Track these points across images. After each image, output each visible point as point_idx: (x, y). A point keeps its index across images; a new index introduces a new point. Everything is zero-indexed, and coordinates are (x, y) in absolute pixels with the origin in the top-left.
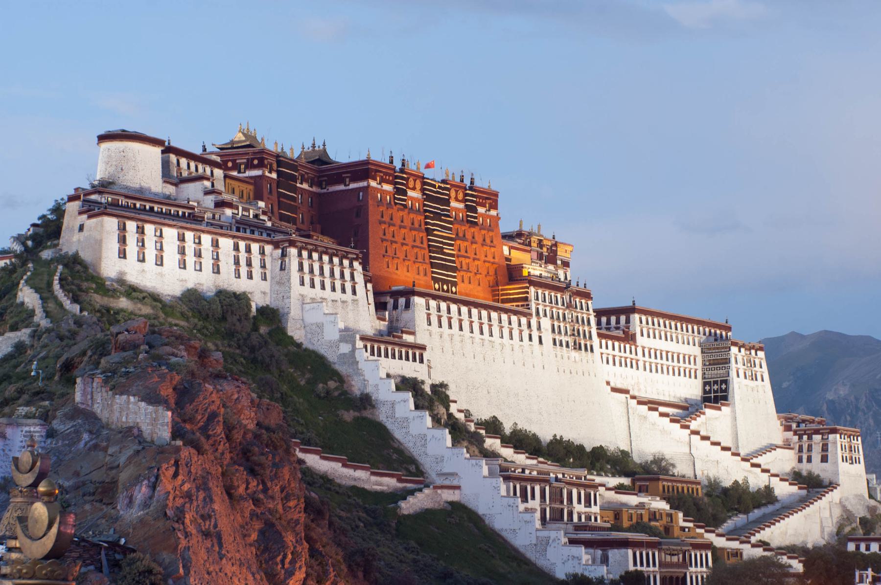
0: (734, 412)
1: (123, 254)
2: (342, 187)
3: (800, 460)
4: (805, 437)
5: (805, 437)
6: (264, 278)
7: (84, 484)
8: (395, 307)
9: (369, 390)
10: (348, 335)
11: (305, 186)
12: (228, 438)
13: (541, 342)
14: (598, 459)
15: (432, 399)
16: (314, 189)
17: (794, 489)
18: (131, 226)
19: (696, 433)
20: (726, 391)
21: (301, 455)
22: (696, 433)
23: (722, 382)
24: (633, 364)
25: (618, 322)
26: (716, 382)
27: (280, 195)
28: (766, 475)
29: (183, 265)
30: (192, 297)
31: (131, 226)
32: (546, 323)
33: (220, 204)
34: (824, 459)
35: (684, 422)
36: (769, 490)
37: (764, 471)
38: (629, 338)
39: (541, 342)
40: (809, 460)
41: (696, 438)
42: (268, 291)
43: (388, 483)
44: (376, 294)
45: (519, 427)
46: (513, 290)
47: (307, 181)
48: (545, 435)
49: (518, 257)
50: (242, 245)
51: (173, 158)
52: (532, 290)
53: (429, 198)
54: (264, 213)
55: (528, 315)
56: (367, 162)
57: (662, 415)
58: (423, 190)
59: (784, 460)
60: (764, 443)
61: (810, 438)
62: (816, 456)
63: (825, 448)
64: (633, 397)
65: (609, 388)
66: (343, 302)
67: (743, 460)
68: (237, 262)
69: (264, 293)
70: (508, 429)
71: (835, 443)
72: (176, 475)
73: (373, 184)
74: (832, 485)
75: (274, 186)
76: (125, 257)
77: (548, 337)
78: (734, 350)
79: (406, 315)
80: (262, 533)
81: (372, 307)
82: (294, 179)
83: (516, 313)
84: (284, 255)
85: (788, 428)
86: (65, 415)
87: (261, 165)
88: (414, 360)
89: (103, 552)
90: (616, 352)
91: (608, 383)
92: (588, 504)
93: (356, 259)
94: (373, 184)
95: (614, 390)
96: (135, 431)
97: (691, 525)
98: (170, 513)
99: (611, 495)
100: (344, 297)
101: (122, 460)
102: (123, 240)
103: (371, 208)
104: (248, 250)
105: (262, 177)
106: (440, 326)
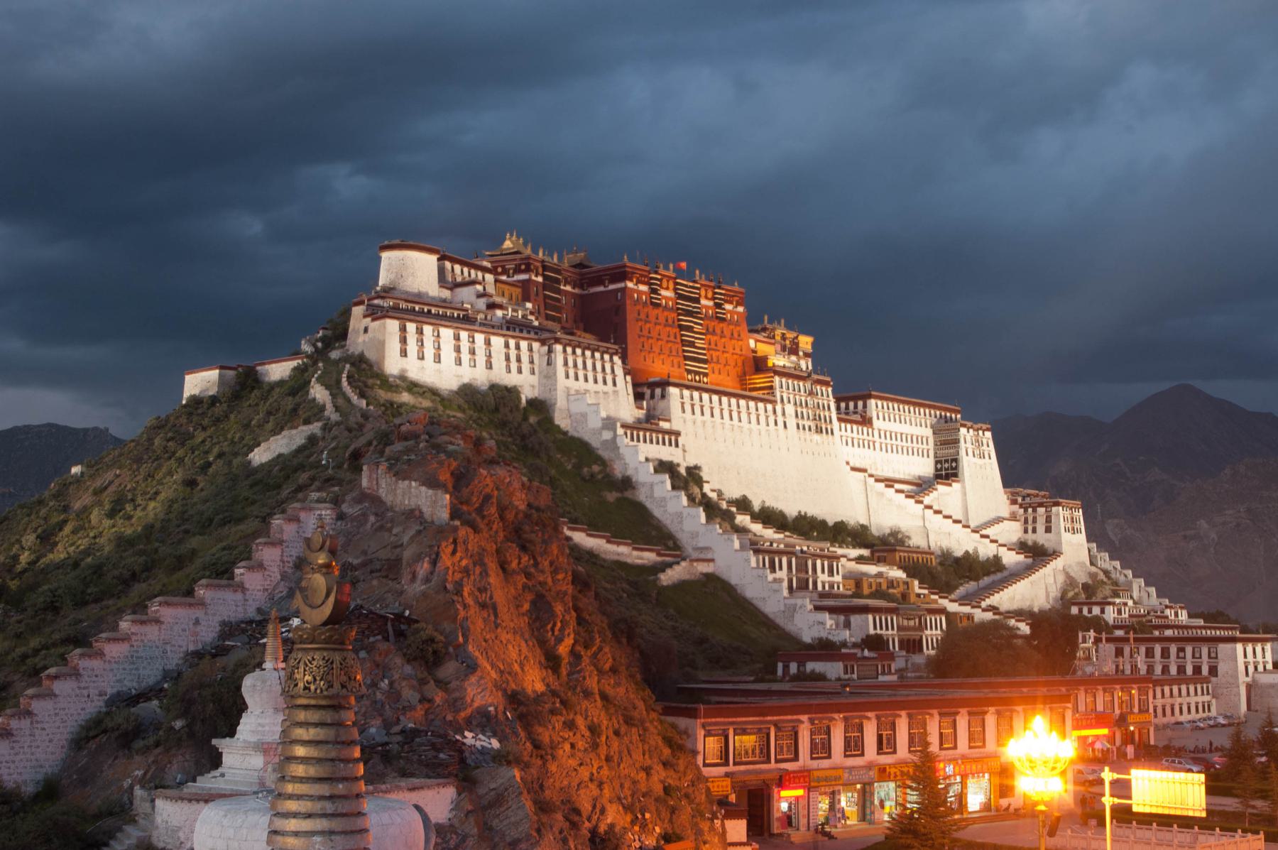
0: (964, 488)
1: (404, 353)
2: (601, 289)
3: (1026, 531)
4: (1030, 510)
5: (1030, 510)
6: (533, 373)
7: (371, 561)
8: (652, 397)
9: (629, 472)
10: (609, 423)
11: (568, 288)
12: (502, 518)
14: (840, 533)
15: (688, 480)
16: (576, 291)
17: (1021, 558)
18: (411, 327)
19: (929, 507)
20: (956, 468)
21: (568, 533)
22: (929, 507)
23: (953, 460)
24: (871, 445)
25: (856, 407)
26: (946, 461)
27: (546, 297)
28: (995, 545)
29: (459, 362)
30: (467, 392)
31: (411, 327)
32: (790, 409)
33: (492, 306)
34: (1048, 530)
35: (917, 498)
36: (997, 559)
37: (992, 541)
38: (866, 421)
40: (1034, 531)
41: (929, 512)
42: (536, 384)
43: (649, 557)
44: (635, 385)
45: (767, 504)
46: (760, 380)
48: (791, 509)
49: (763, 349)
50: (512, 342)
51: (448, 265)
52: (777, 379)
53: (680, 297)
54: (532, 313)
55: (774, 402)
57: (898, 491)
58: (675, 289)
59: (1011, 531)
60: (993, 515)
62: (1041, 528)
63: (1048, 520)
64: (871, 476)
65: (848, 468)
66: (605, 393)
67: (974, 531)
68: (508, 359)
69: (533, 386)
70: (756, 506)
71: (1058, 515)
72: (454, 552)
73: (630, 285)
74: (1055, 554)
75: (540, 289)
76: (406, 356)
77: (792, 422)
79: (662, 404)
80: (533, 603)
81: (631, 398)
82: (558, 281)
83: (762, 400)
84: (550, 351)
85: (1014, 502)
86: (353, 499)
87: (528, 270)
89: (389, 624)
90: (855, 434)
92: (831, 573)
93: (616, 354)
94: (630, 285)
95: (854, 469)
96: (417, 513)
97: (926, 592)
98: (450, 586)
99: (853, 566)
100: (605, 388)
101: (406, 539)
102: (404, 340)
103: (628, 307)
104: (518, 347)
105: (529, 280)
106: (693, 413)
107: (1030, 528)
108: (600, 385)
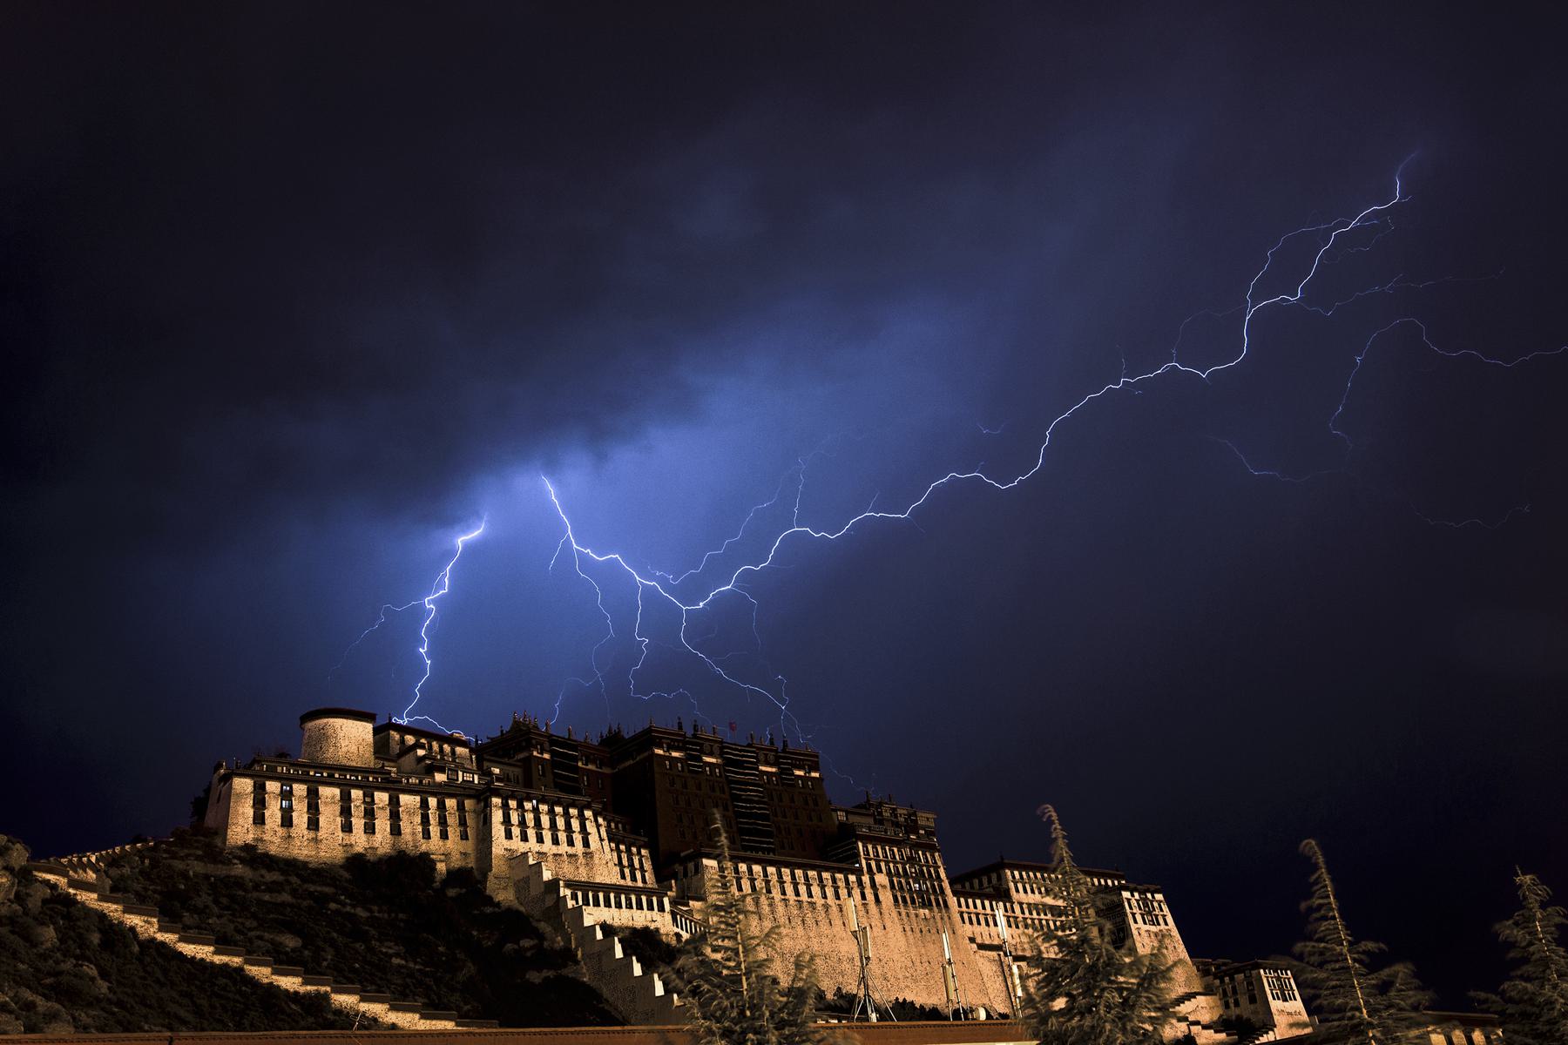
3: (1227, 1006)
4: (1227, 979)
5: (1227, 979)
6: (464, 837)
8: (686, 875)
10: (553, 885)
11: (590, 767)
13: (877, 901)
16: (606, 770)
25: (990, 881)
29: (347, 828)
32: (881, 879)
37: (1180, 1020)
39: (877, 901)
40: (1237, 1004)
47: (593, 762)
51: (396, 736)
53: (728, 762)
56: (649, 730)
61: (1232, 979)
62: (1244, 1000)
66: (570, 856)
68: (425, 821)
77: (886, 897)
78: (1126, 894)
88: (651, 908)
91: (972, 940)
93: (588, 807)
95: (982, 947)
107: (1231, 1001)
108: (564, 848)
